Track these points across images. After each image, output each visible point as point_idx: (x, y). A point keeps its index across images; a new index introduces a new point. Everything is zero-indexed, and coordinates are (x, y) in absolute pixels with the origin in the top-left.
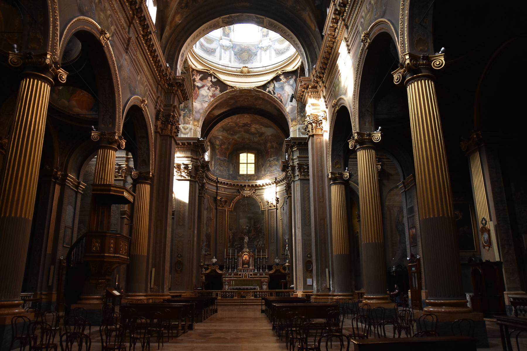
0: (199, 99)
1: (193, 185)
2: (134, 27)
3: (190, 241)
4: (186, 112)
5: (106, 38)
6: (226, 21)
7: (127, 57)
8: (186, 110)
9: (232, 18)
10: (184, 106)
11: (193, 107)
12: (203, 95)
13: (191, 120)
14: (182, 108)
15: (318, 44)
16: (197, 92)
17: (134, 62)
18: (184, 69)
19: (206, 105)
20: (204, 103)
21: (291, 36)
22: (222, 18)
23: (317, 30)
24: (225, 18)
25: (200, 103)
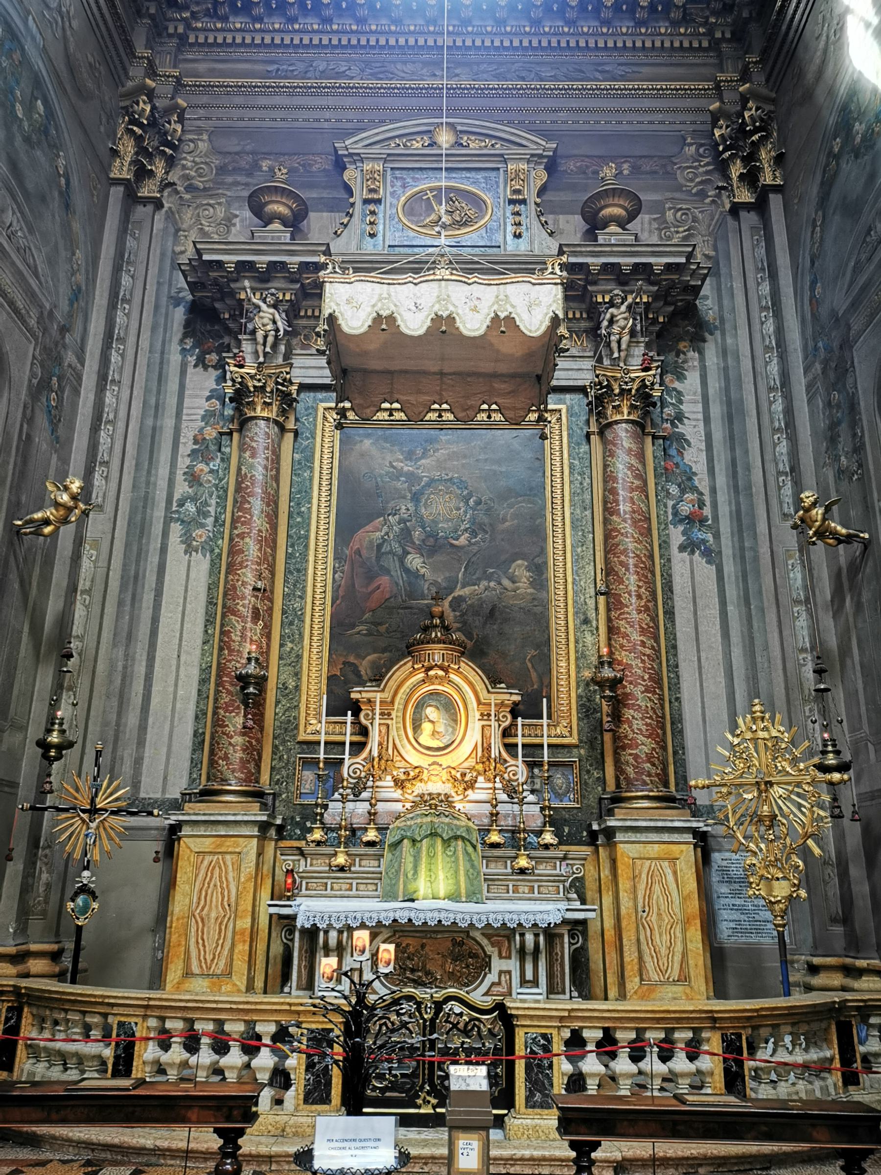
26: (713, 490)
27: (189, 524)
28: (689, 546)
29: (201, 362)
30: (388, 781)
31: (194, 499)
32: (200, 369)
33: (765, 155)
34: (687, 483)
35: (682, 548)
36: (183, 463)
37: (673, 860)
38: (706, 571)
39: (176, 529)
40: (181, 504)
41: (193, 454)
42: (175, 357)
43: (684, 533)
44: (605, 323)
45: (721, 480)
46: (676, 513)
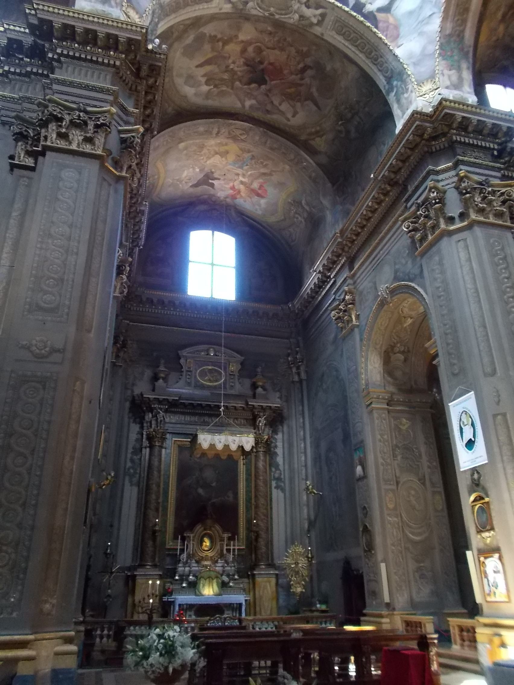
0: (403, 31)
1: (465, 240)
3: (504, 415)
4: (397, 86)
8: (395, 83)
10: (386, 80)
11: (399, 61)
12: (411, 13)
13: (412, 92)
14: (387, 87)
16: (387, 21)
18: (310, 9)
19: (436, 24)
20: (427, 23)
25: (416, 35)
26: (284, 470)
27: (131, 476)
28: (277, 487)
29: (135, 422)
30: (194, 561)
31: (132, 468)
32: (134, 424)
33: (302, 368)
34: (277, 467)
35: (275, 488)
36: (129, 456)
37: (270, 582)
38: (281, 495)
39: (127, 478)
40: (129, 469)
41: (133, 453)
42: (126, 419)
43: (276, 483)
44: (258, 422)
45: (287, 467)
46: (274, 477)
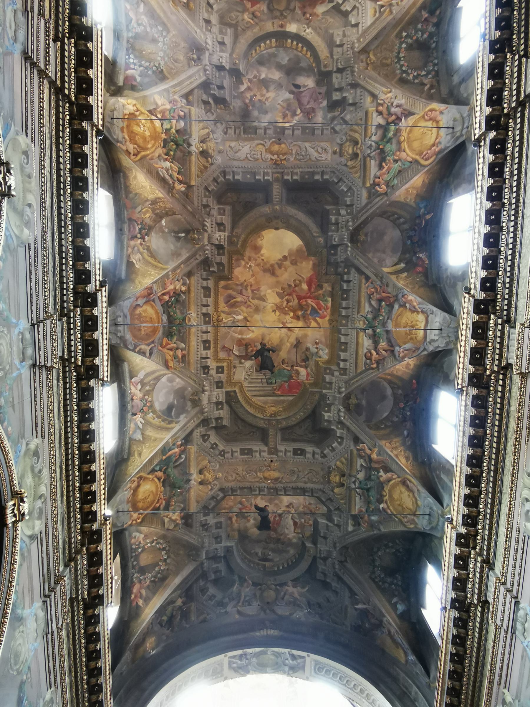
2: (76, 570)
5: (19, 512)
6: (235, 665)
7: (41, 614)
9: (247, 659)
15: (418, 688)
17: (49, 636)
21: (360, 687)
22: (229, 657)
23: (412, 658)
24: (234, 657)
